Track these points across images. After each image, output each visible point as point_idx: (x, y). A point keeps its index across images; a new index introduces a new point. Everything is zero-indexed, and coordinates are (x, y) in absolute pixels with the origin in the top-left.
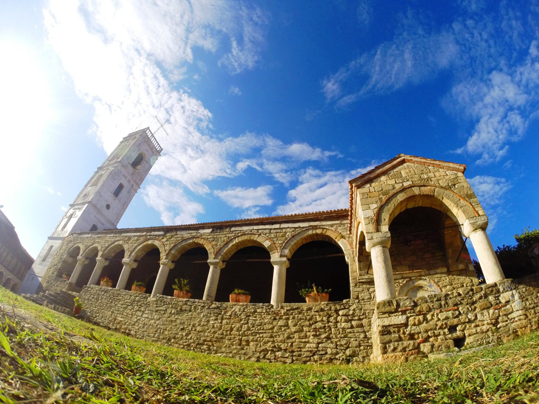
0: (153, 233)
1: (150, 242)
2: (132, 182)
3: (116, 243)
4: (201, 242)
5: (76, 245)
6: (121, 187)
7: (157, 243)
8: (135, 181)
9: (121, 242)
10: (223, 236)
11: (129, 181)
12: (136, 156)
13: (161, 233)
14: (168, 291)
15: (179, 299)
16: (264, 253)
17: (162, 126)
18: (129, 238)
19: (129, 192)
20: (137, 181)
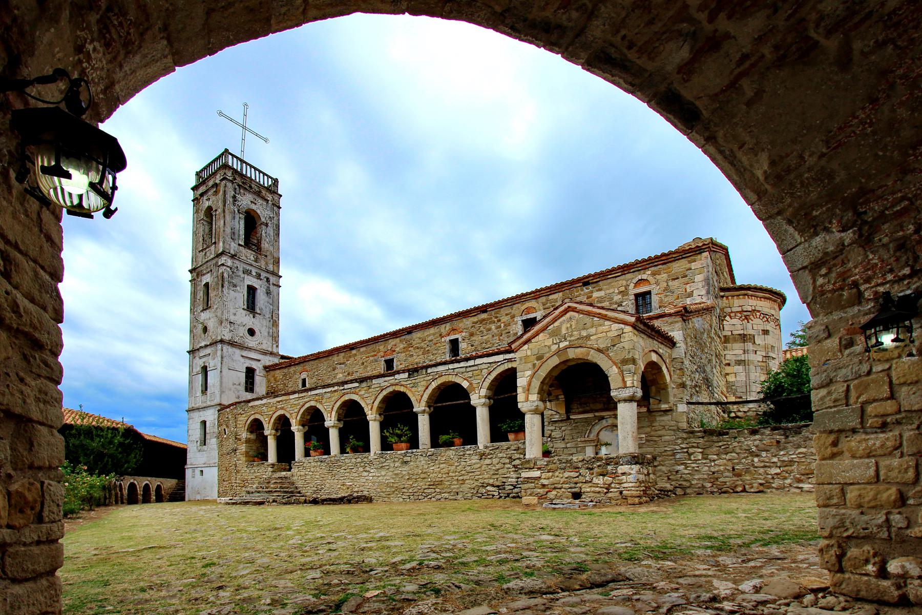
0: (346, 386)
1: (346, 398)
2: (263, 275)
3: (307, 405)
4: (402, 389)
5: (252, 418)
6: (252, 290)
7: (354, 397)
8: (268, 272)
9: (313, 403)
10: (421, 379)
11: (258, 276)
12: (242, 223)
13: (356, 385)
14: (386, 446)
15: (400, 452)
16: (463, 394)
17: (244, 127)
18: (322, 395)
19: (268, 293)
20: (271, 268)
